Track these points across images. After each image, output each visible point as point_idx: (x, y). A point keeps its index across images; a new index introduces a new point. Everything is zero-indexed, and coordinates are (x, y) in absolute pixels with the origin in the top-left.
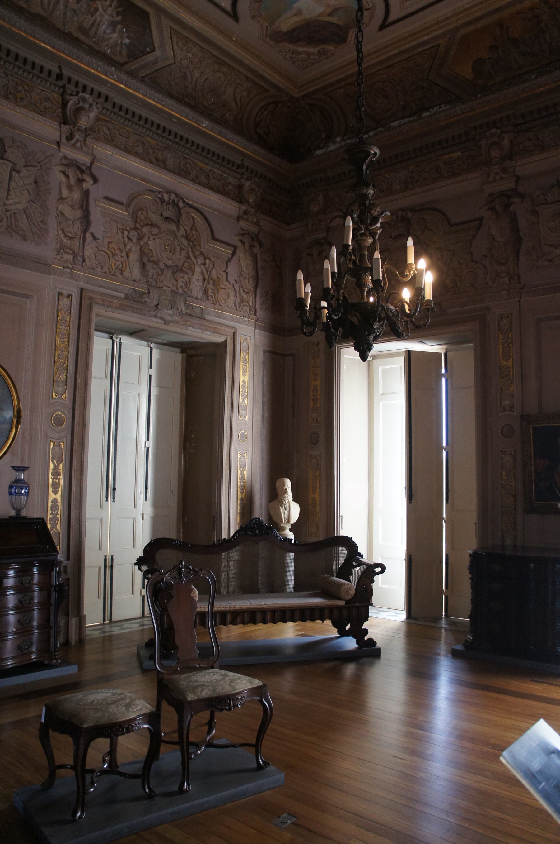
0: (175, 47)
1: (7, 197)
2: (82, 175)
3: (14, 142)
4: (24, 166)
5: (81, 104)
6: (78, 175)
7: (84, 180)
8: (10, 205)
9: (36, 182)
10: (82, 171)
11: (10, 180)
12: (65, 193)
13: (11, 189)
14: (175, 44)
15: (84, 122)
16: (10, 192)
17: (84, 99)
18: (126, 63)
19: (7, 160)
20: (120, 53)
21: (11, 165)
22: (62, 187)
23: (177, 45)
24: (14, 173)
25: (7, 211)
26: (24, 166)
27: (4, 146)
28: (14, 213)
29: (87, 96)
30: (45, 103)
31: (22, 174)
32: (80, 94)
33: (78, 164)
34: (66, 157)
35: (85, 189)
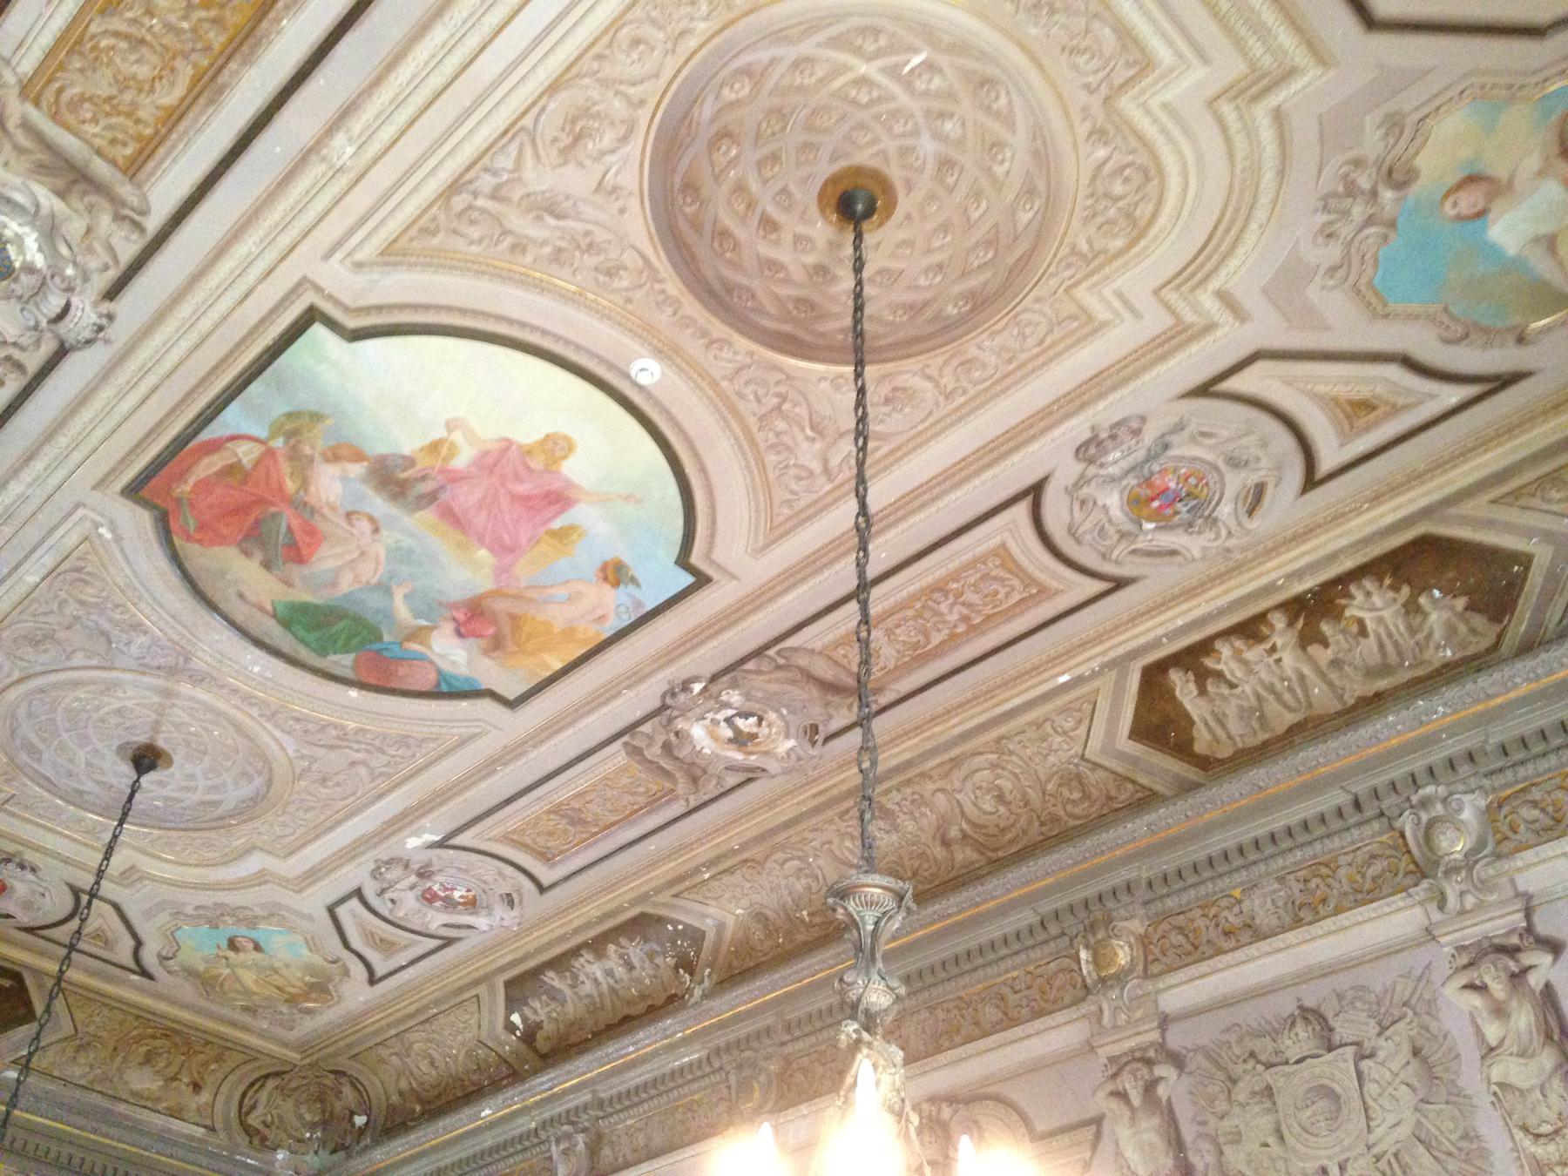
0: (1555, 508)
1: (1369, 1126)
2: (1517, 961)
3: (1340, 997)
4: (1379, 1034)
5: (1425, 817)
6: (1506, 968)
7: (1525, 970)
8: (1381, 1140)
9: (1416, 1052)
10: (1513, 951)
11: (1361, 1086)
12: (1493, 1032)
13: (1370, 1102)
14: (1545, 506)
15: (1455, 845)
16: (1371, 1113)
17: (1425, 803)
18: (1500, 637)
19: (1341, 1046)
20: (1473, 631)
21: (1349, 1051)
22: (1479, 1022)
23: (1550, 501)
24: (1365, 1065)
25: (1378, 1158)
26: (1379, 1034)
27: (1325, 1019)
28: (1396, 1155)
29: (1429, 790)
30: (1371, 872)
31: (1381, 1054)
32: (1414, 799)
33: (1496, 941)
34: (1461, 949)
35: (1538, 990)
